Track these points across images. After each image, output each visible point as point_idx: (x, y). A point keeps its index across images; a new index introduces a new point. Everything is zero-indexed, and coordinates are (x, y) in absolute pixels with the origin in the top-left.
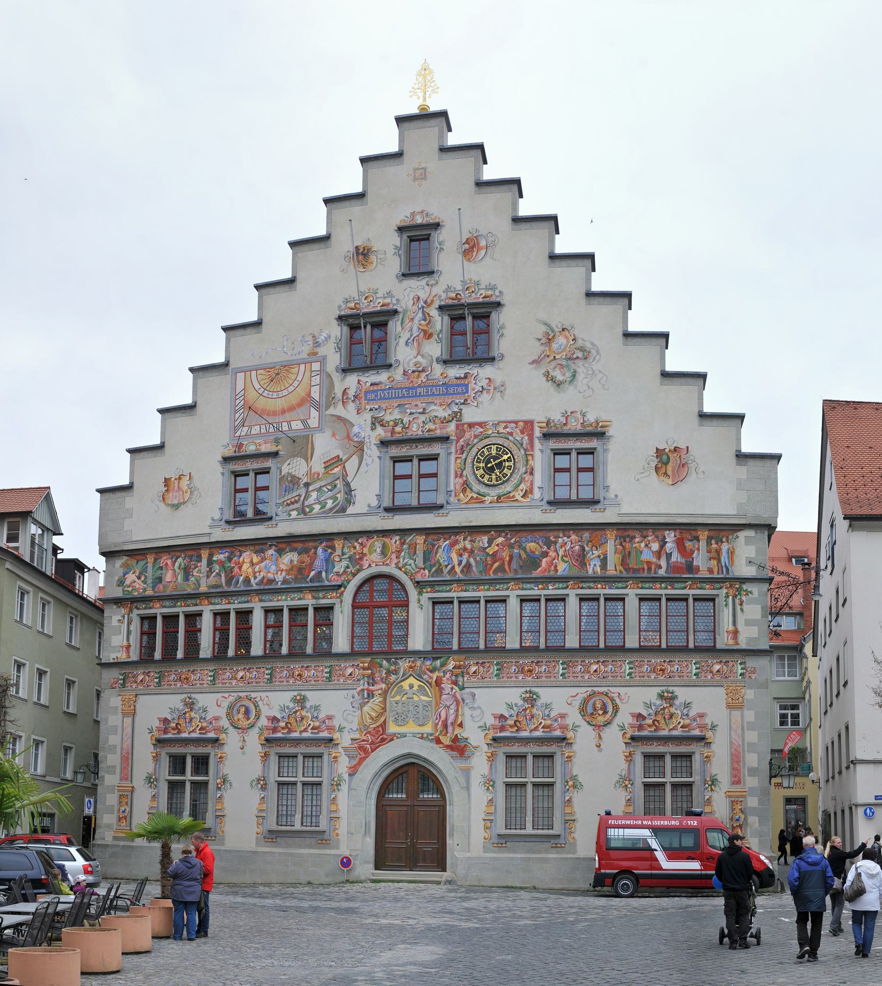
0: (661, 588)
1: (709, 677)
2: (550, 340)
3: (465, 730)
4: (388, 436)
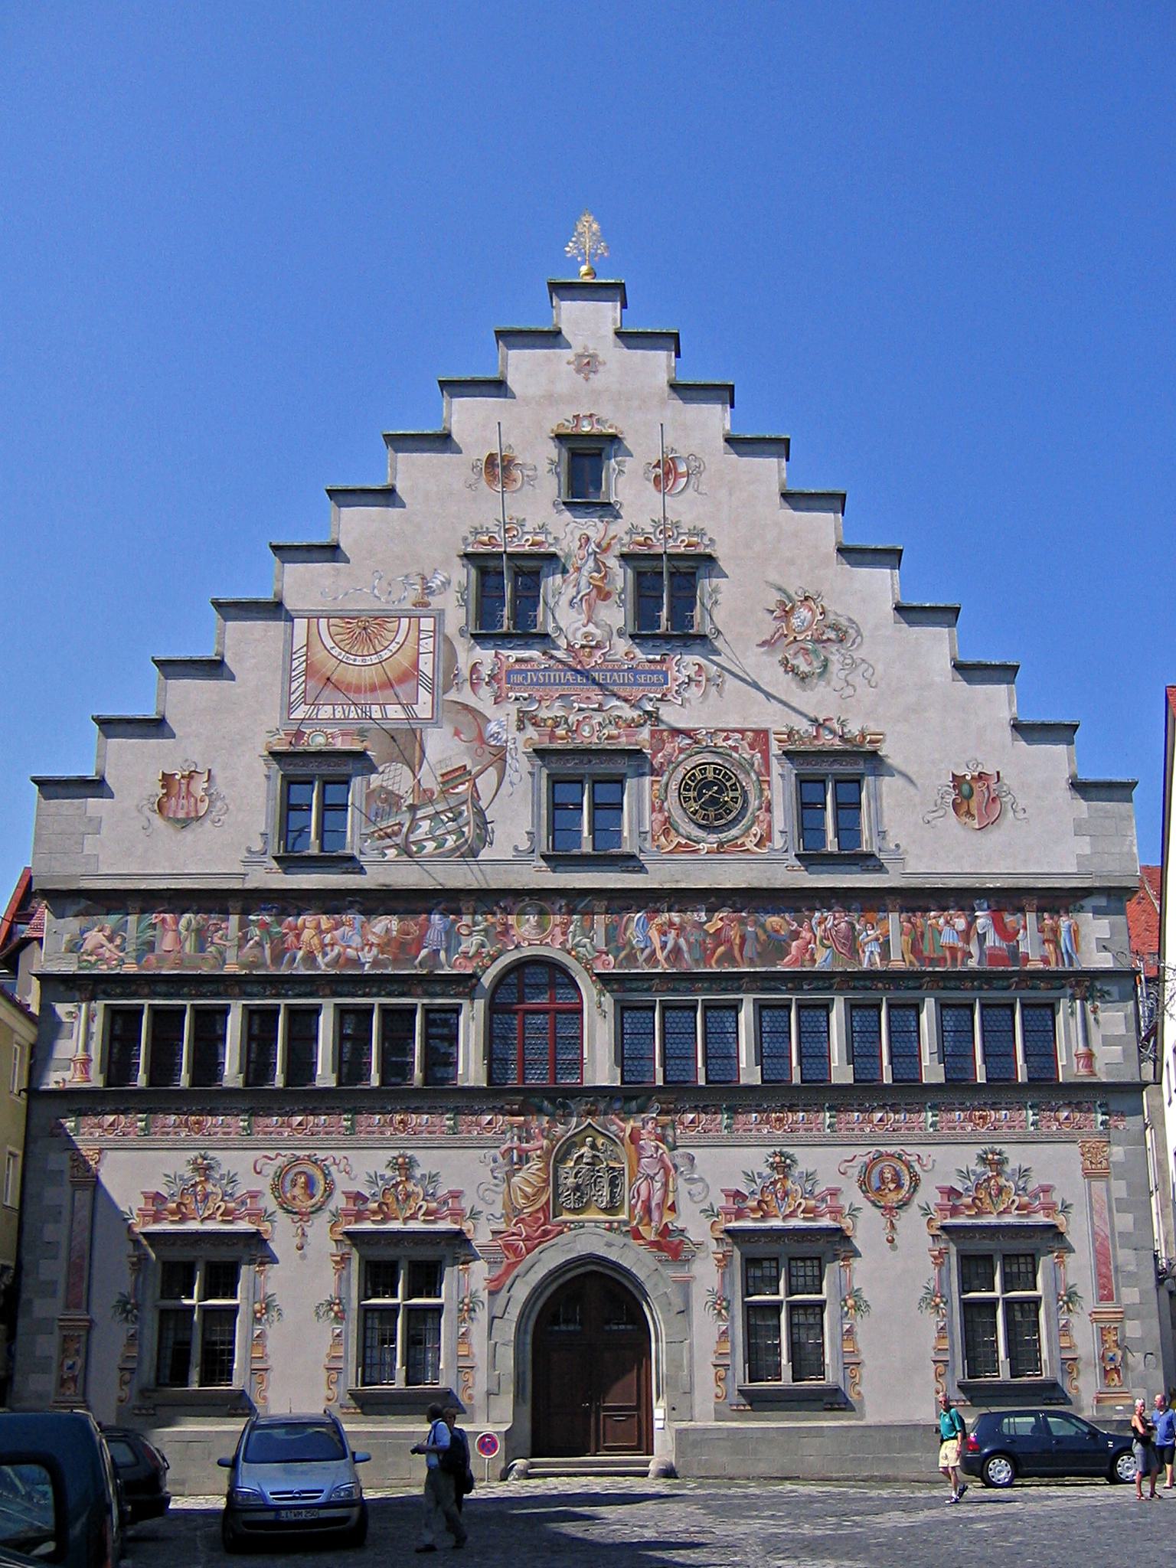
0: (973, 989)
1: (1054, 1128)
2: (787, 614)
3: (679, 1215)
4: (546, 744)
